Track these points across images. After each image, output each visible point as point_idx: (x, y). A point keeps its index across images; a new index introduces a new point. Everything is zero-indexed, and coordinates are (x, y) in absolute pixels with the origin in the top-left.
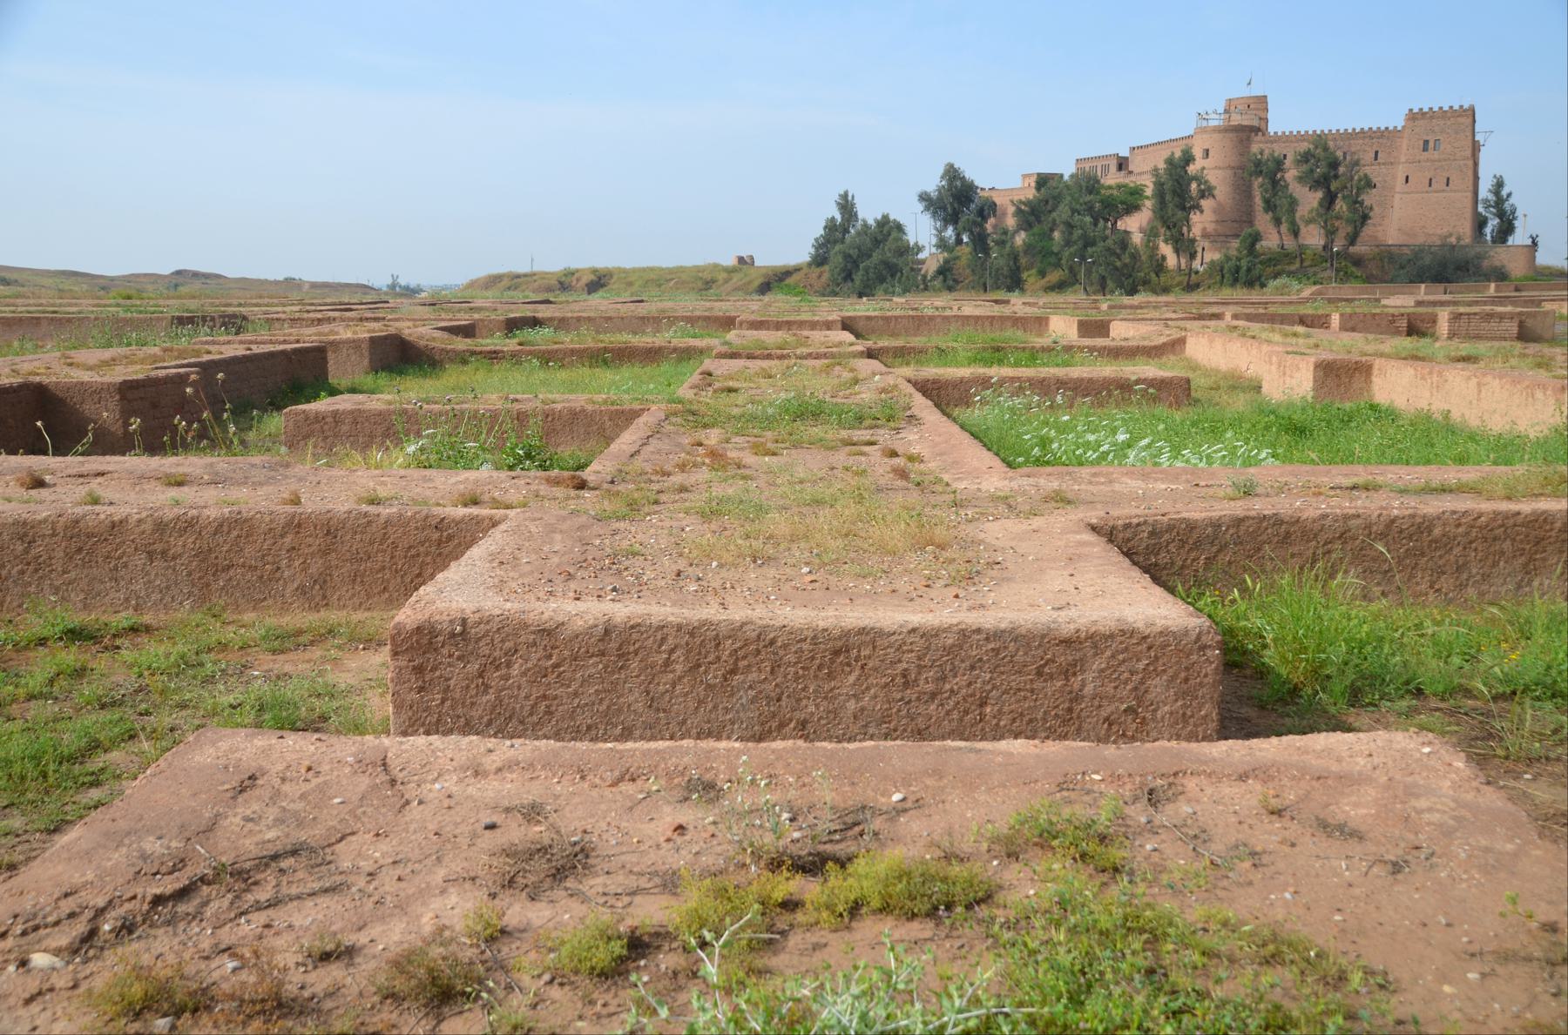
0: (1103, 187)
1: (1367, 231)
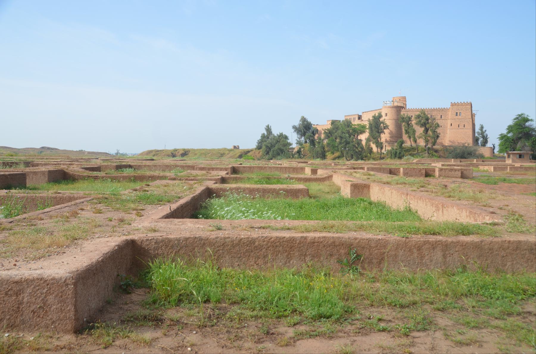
0: (353, 125)
1: (439, 141)
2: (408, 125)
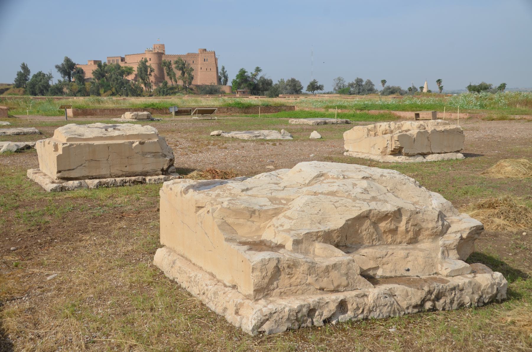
1: (193, 82)
2: (169, 68)
